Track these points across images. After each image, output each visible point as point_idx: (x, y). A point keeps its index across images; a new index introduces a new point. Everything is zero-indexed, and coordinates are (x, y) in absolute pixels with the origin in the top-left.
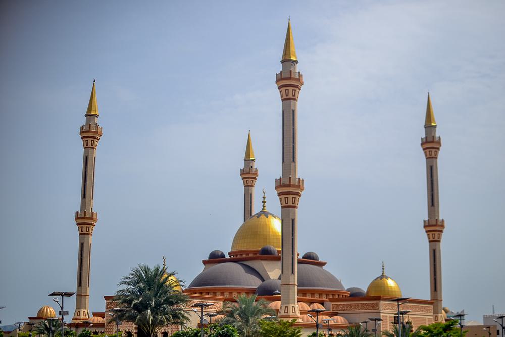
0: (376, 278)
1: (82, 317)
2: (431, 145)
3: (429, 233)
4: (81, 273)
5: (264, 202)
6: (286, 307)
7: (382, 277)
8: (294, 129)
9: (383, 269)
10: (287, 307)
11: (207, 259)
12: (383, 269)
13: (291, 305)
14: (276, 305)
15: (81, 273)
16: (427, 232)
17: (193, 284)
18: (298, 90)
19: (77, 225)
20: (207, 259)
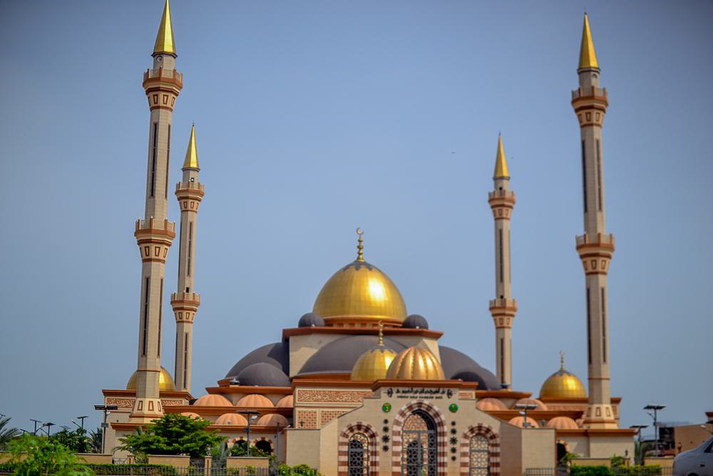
0: (551, 374)
1: (146, 411)
2: (499, 203)
3: (495, 317)
4: (145, 331)
5: (360, 248)
6: (598, 408)
7: (562, 372)
8: (599, 166)
9: (562, 362)
10: (598, 408)
11: (297, 327)
12: (562, 362)
13: (595, 406)
14: (287, 403)
15: (145, 331)
16: (494, 315)
17: (304, 369)
18: (602, 113)
19: (139, 244)
20: (297, 327)
